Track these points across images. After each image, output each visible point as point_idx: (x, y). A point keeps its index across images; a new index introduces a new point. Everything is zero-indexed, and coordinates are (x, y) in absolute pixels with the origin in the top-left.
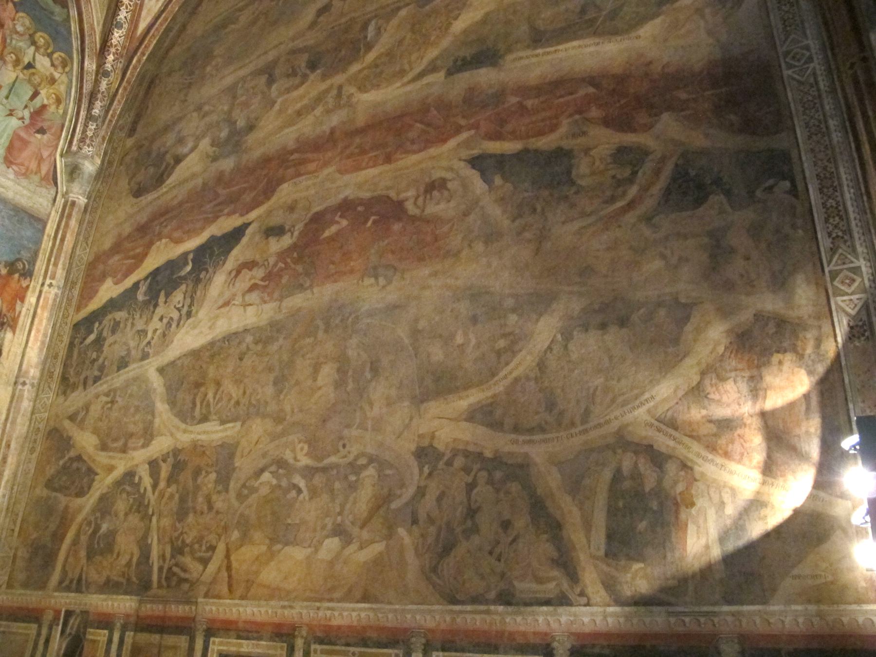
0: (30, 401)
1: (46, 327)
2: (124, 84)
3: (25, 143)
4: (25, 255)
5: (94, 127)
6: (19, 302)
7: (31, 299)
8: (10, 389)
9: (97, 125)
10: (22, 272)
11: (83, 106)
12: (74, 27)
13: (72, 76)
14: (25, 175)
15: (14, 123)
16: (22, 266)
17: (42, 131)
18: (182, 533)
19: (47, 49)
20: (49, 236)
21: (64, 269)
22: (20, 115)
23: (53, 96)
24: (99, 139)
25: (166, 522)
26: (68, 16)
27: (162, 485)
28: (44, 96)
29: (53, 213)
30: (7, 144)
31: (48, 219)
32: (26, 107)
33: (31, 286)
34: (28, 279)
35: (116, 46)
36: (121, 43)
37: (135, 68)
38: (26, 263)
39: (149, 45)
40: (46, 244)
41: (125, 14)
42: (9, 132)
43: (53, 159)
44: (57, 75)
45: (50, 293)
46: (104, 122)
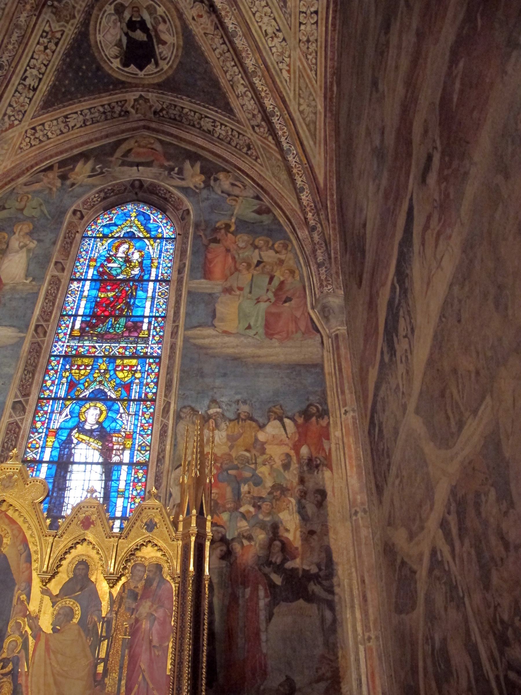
0: (368, 528)
1: (356, 449)
2: (331, 225)
3: (278, 316)
4: (313, 399)
5: (324, 270)
6: (325, 441)
7: (336, 433)
8: (348, 524)
9: (326, 268)
10: (318, 414)
11: (311, 263)
12: (282, 220)
13: (295, 250)
14: (288, 337)
15: (263, 306)
16: (315, 409)
17: (288, 300)
18: (496, 607)
19: (268, 244)
20: (329, 374)
21: (351, 393)
22: (265, 298)
23: (287, 271)
24: (334, 276)
25: (477, 597)
26: (275, 216)
27: (457, 544)
28: (279, 277)
29: (325, 354)
30: (264, 323)
31: (323, 361)
32: (268, 290)
33: (331, 422)
34: (326, 417)
35: (308, 205)
36: (311, 200)
37: (332, 209)
38: (318, 405)
39: (332, 186)
40: (330, 382)
41: (300, 179)
42: (262, 314)
43: (306, 314)
44: (283, 257)
45: (347, 419)
46: (330, 263)
